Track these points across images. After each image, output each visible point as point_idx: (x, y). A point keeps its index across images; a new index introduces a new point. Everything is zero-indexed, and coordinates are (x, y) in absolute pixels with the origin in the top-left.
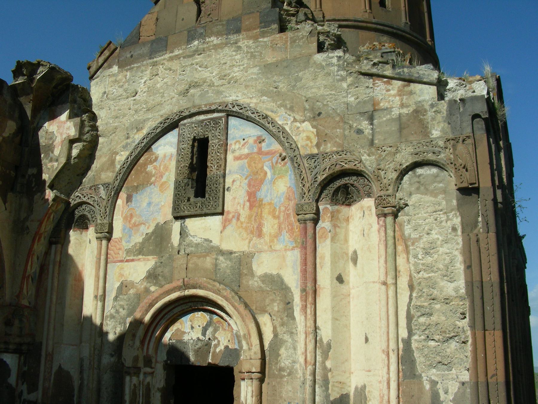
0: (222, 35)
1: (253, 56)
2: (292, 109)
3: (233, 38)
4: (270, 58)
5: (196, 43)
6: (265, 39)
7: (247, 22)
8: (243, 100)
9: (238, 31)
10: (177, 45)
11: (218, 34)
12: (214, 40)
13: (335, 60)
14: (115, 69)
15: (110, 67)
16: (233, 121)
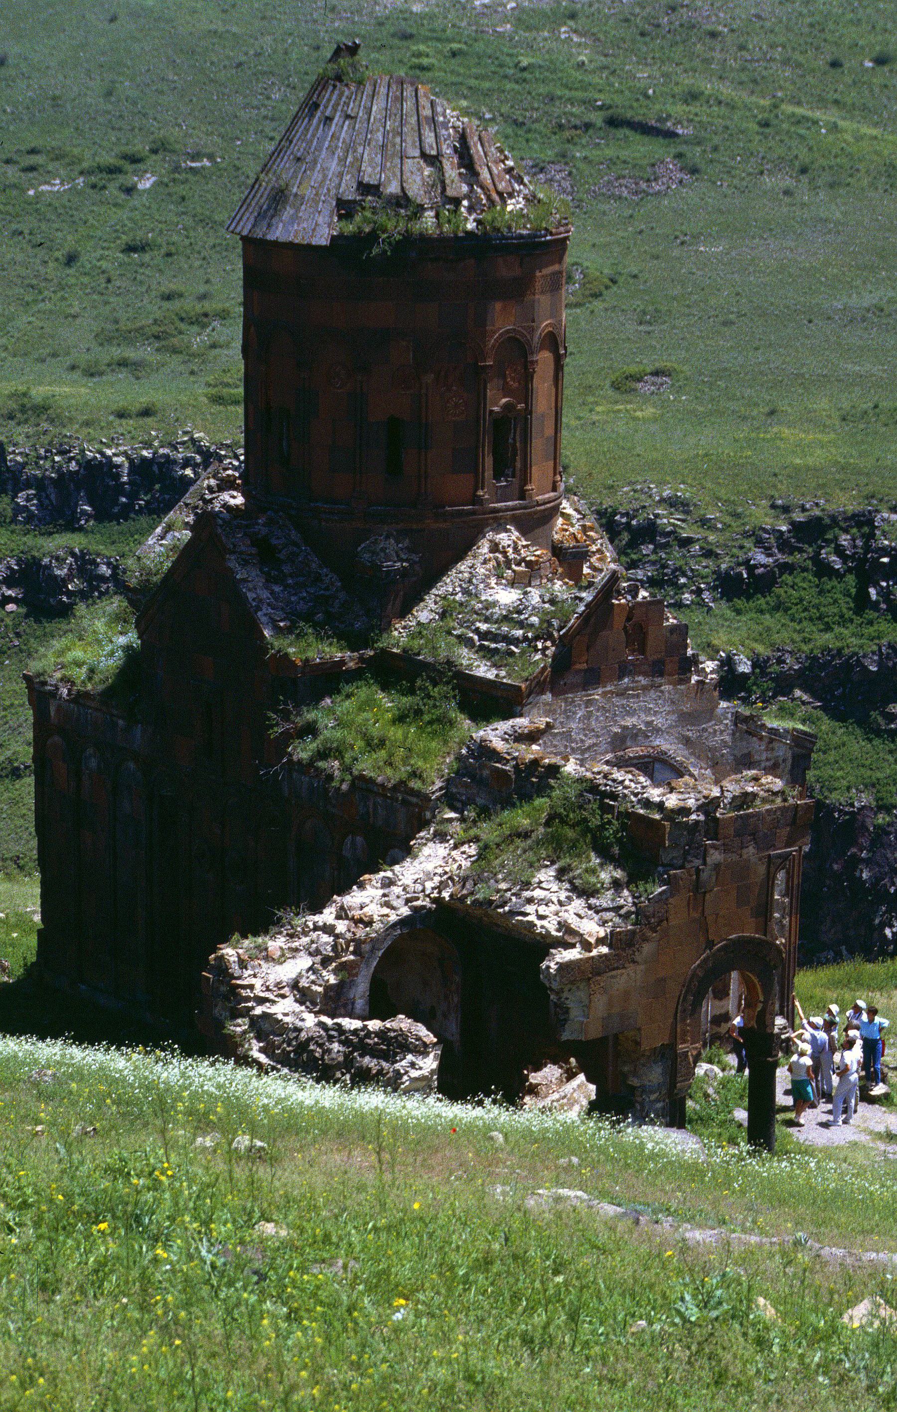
0: (648, 676)
1: (673, 702)
2: (699, 757)
3: (658, 680)
4: (687, 707)
5: (626, 680)
6: (682, 687)
7: (669, 667)
8: (665, 747)
9: (661, 675)
10: (610, 680)
11: (645, 674)
12: (643, 680)
13: (729, 716)
14: (548, 697)
15: (542, 692)
16: (657, 766)
